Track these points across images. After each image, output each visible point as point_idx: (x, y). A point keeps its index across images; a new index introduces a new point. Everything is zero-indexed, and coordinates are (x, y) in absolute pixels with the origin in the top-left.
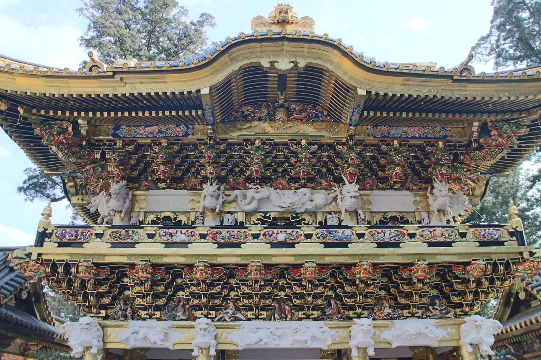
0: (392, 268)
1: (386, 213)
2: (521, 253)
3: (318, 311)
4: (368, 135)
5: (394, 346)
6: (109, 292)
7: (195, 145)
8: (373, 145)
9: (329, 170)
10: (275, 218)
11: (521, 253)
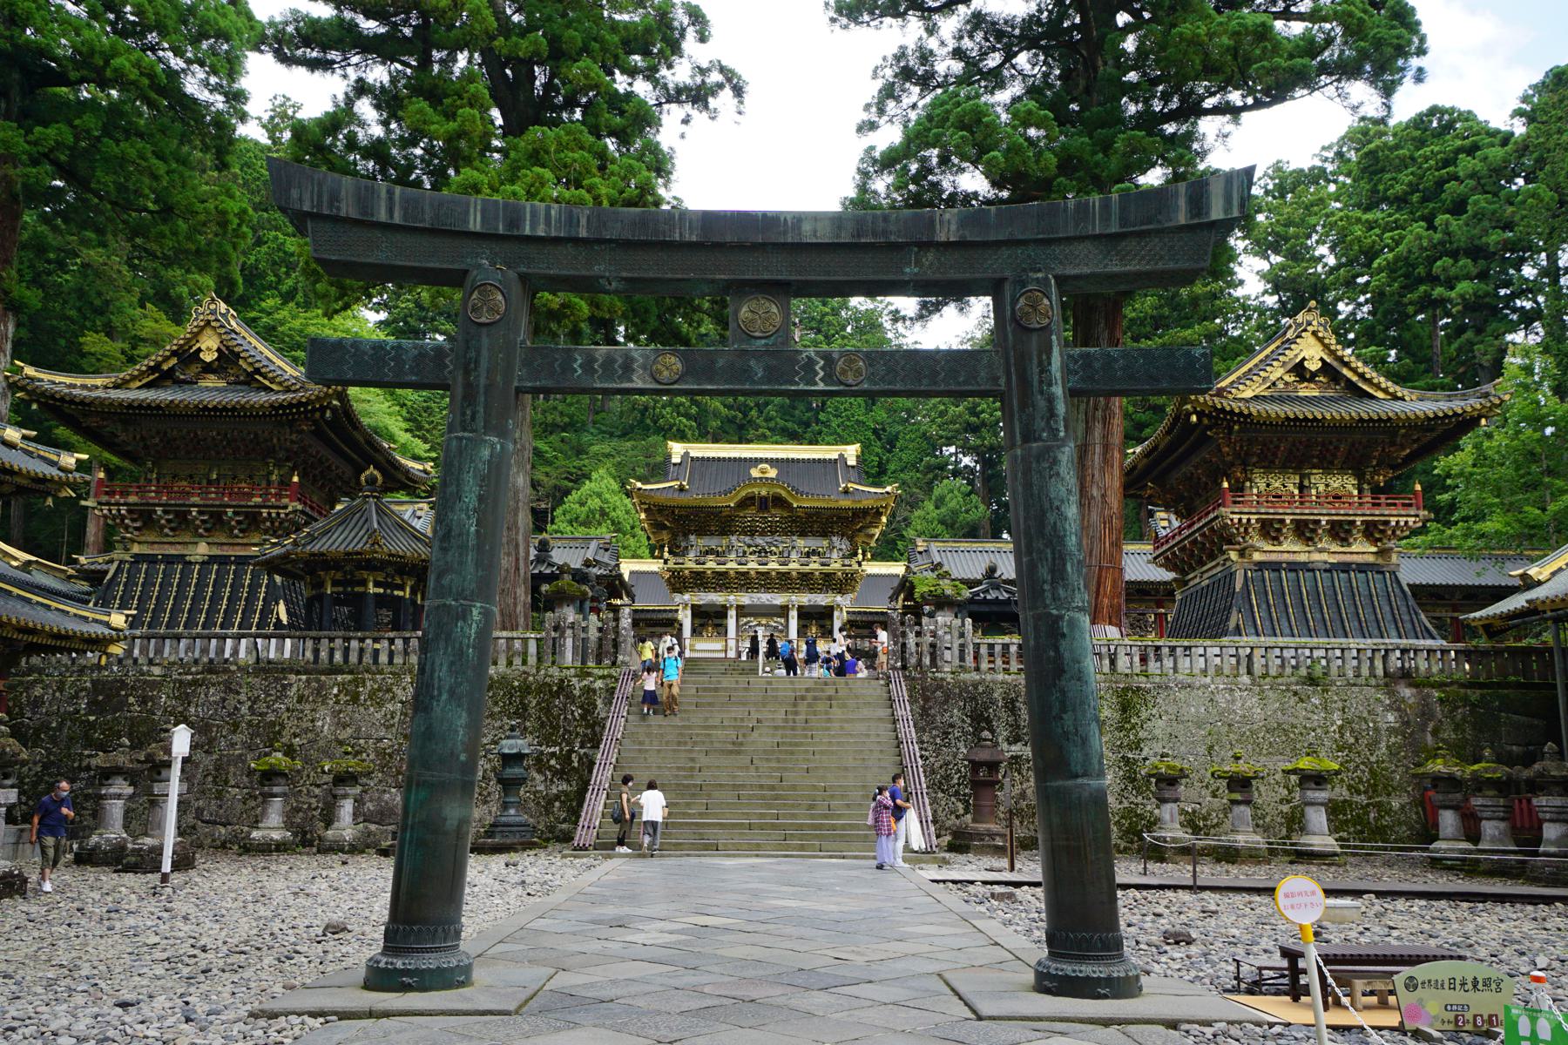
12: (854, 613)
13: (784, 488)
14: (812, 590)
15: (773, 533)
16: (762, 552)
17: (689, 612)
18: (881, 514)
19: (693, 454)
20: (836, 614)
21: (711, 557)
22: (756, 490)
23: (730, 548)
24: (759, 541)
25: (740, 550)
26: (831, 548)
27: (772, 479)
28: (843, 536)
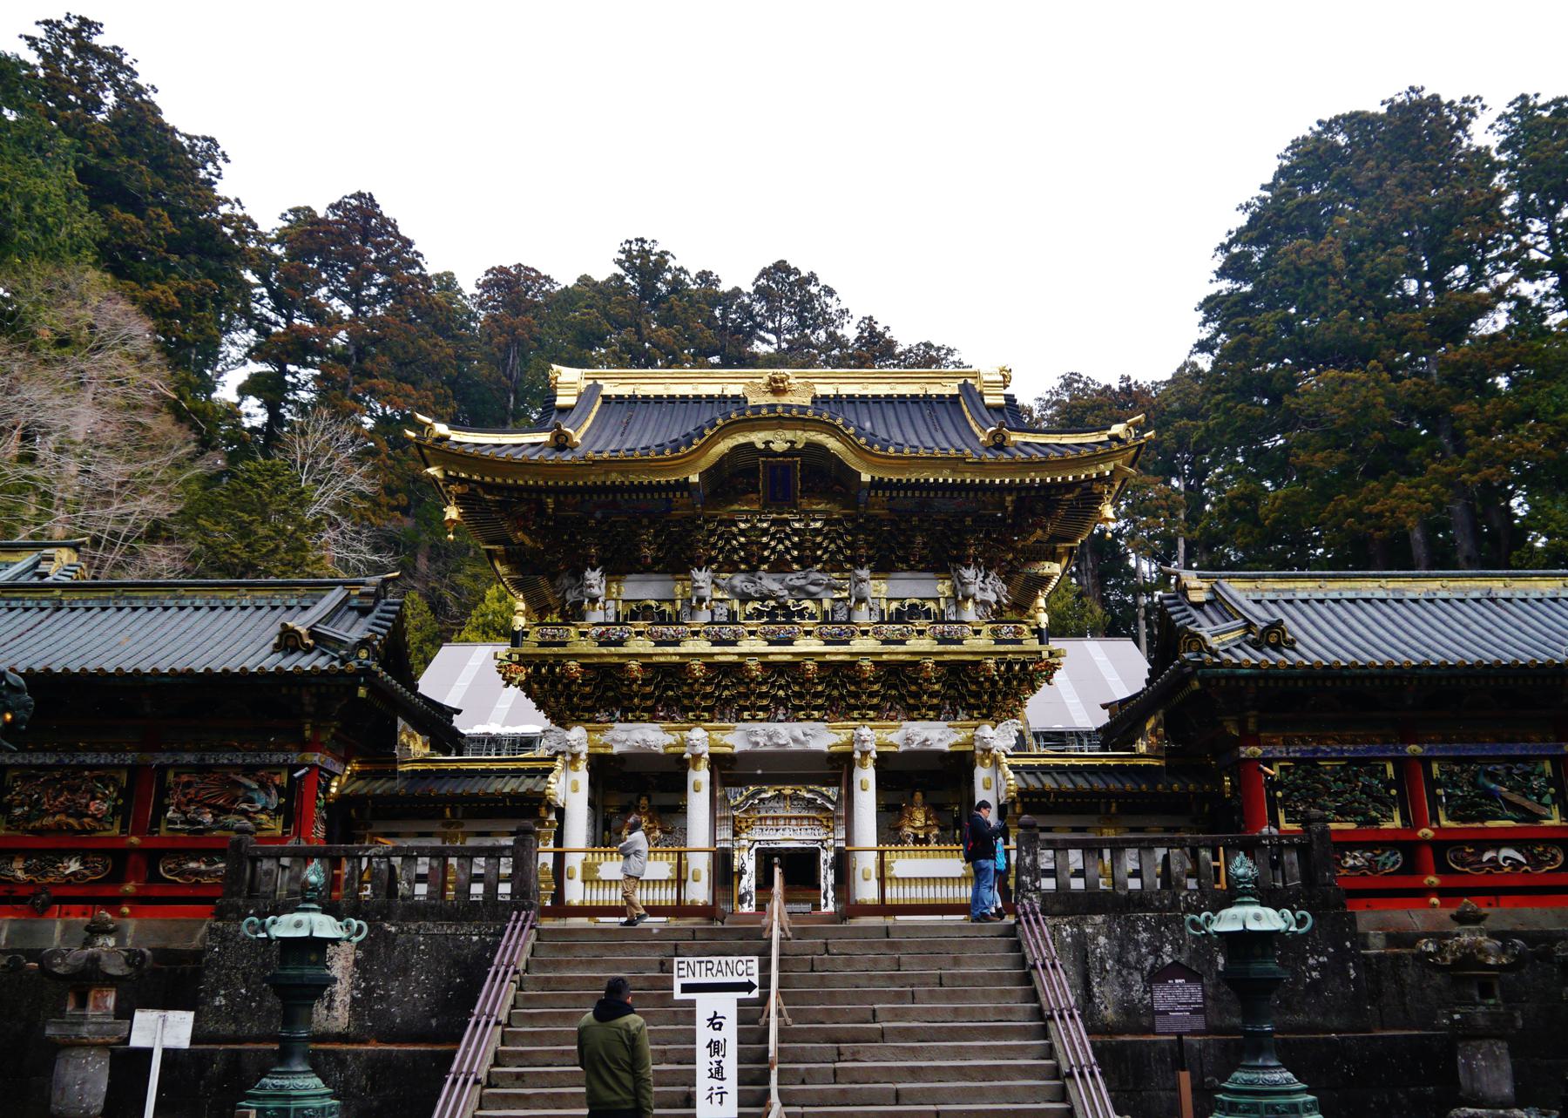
2: (1040, 653)
5: (901, 749)
6: (593, 693)
7: (679, 521)
9: (838, 547)
11: (1040, 653)
12: (1030, 770)
13: (833, 430)
14: (914, 711)
15: (806, 563)
16: (780, 615)
17: (582, 776)
18: (1099, 499)
19: (609, 389)
20: (981, 773)
21: (641, 625)
22: (758, 438)
23: (694, 604)
24: (770, 583)
25: (722, 613)
28: (988, 568)
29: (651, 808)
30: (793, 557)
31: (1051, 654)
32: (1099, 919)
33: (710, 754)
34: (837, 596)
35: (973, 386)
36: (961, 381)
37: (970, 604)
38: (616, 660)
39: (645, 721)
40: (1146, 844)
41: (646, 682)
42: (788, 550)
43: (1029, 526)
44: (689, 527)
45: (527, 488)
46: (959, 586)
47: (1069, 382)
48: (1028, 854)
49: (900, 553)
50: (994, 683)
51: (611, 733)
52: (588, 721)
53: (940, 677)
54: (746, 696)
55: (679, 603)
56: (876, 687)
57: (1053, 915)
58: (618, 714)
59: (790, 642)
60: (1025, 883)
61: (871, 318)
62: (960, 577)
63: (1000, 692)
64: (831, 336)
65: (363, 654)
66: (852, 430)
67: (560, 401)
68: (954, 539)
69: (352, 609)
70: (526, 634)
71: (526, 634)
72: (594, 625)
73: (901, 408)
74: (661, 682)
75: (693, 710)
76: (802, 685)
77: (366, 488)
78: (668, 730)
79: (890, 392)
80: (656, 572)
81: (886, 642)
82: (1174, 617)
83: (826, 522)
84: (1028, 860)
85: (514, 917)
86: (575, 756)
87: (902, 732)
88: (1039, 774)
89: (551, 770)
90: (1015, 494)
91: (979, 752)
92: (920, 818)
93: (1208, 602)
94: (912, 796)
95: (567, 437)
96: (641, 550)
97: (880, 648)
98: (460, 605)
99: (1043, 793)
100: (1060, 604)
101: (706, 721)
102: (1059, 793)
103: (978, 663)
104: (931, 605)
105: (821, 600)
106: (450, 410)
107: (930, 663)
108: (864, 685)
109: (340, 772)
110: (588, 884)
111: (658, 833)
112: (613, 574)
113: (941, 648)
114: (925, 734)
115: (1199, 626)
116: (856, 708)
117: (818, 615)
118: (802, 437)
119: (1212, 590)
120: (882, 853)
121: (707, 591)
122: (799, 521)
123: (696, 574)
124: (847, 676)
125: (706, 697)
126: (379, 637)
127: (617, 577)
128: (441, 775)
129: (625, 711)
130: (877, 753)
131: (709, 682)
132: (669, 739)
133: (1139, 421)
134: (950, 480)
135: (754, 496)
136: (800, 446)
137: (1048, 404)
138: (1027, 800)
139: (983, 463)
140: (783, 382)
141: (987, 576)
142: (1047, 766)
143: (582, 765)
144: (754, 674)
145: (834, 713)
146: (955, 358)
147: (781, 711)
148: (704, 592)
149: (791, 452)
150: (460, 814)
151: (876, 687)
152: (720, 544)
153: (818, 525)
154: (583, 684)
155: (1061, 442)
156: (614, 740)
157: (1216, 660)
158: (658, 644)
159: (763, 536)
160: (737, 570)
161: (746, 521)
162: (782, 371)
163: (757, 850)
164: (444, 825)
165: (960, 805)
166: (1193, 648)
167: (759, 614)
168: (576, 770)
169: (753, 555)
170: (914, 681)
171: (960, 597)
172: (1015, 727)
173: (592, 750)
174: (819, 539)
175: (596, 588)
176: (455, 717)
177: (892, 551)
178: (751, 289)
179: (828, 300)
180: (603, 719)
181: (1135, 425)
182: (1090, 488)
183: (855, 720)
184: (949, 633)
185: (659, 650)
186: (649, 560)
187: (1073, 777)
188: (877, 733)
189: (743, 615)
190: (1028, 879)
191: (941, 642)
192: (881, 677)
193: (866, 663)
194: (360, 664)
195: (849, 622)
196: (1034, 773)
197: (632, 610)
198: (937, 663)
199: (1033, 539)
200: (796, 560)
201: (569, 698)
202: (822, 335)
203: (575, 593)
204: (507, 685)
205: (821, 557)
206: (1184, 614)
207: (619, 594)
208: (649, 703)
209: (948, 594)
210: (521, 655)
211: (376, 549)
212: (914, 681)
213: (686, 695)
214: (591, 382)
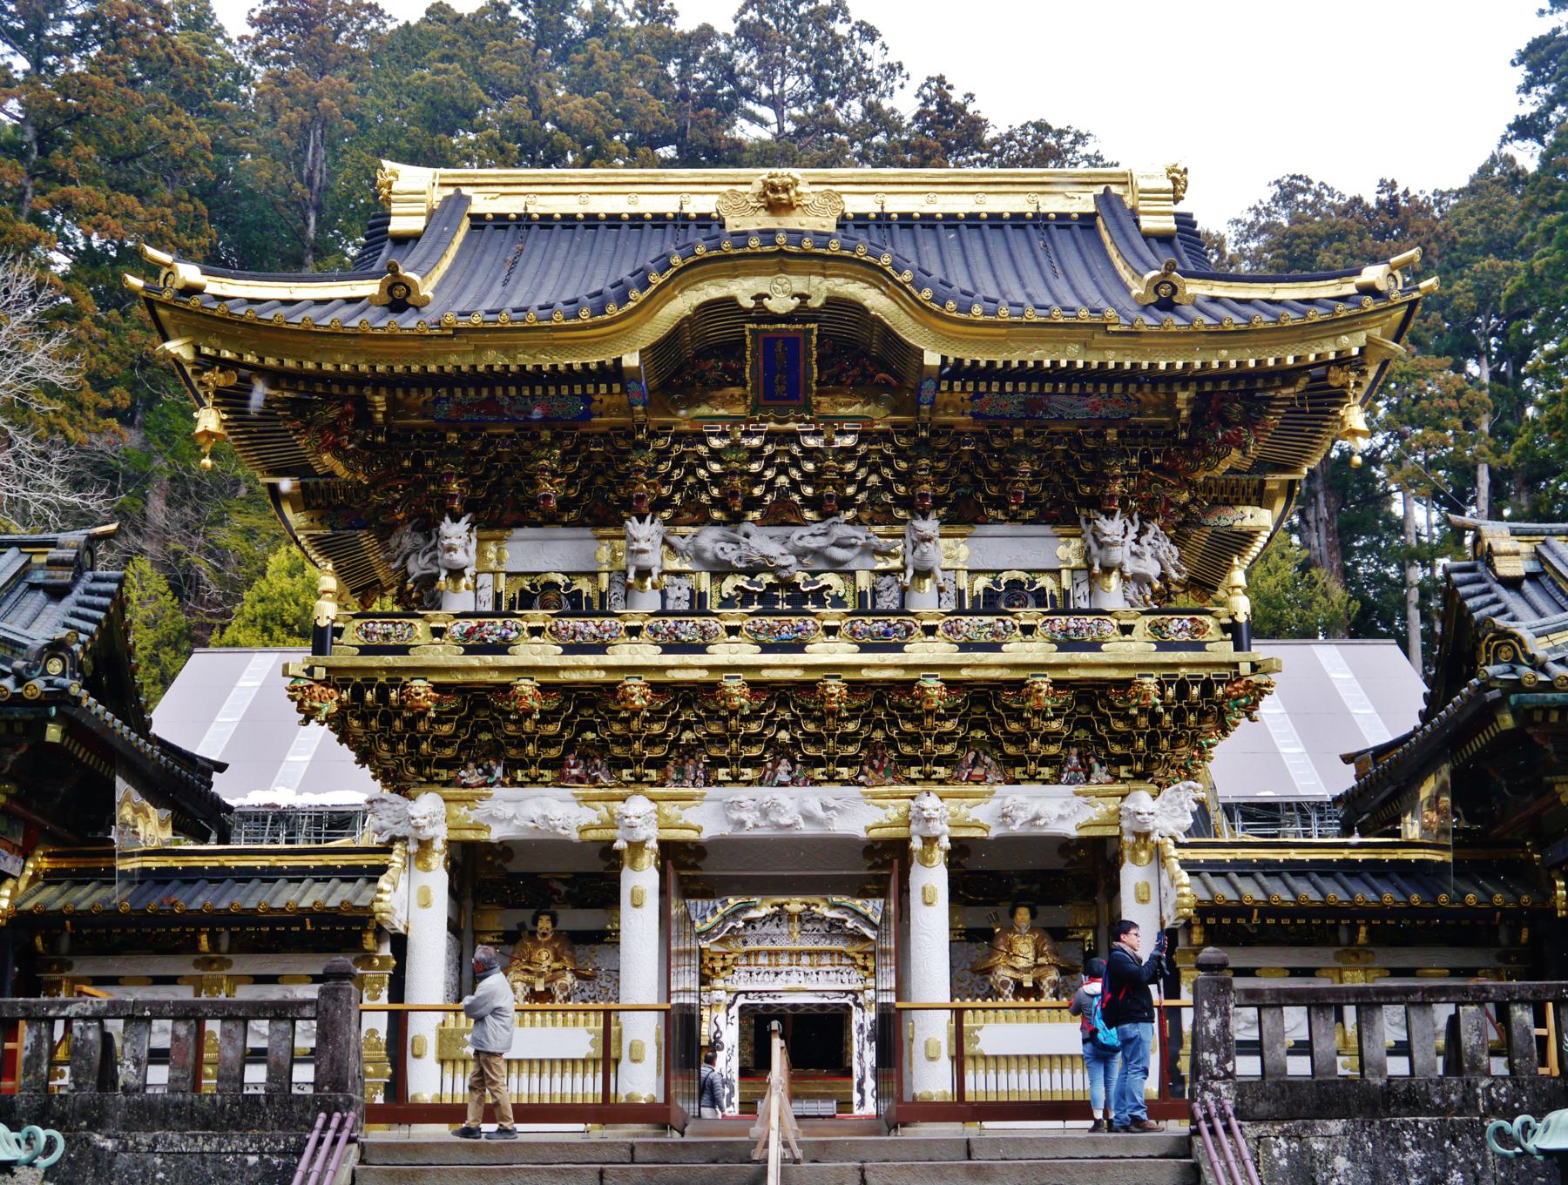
0: (990, 687)
1: (1001, 571)
2: (1236, 665)
3: (850, 767)
4: (963, 414)
5: (994, 833)
6: (455, 736)
7: (602, 435)
8: (973, 433)
9: (884, 480)
10: (769, 585)
11: (1236, 665)
13: (873, 273)
15: (825, 508)
17: (437, 879)
18: (1338, 396)
19: (483, 203)
20: (1132, 876)
21: (538, 617)
22: (743, 290)
24: (764, 542)
25: (679, 597)
26: (1094, 572)
27: (821, 237)
29: (558, 935)
30: (804, 498)
31: (1255, 667)
32: (1336, 1126)
33: (661, 843)
34: (882, 566)
35: (1119, 198)
36: (1100, 190)
37: (1114, 581)
38: (495, 677)
39: (545, 784)
40: (1418, 997)
41: (547, 717)
42: (795, 486)
43: (1219, 444)
44: (622, 444)
45: (338, 378)
46: (1094, 549)
47: (1288, 191)
48: (1213, 1015)
49: (993, 491)
50: (1155, 718)
51: (486, 804)
52: (446, 784)
53: (1061, 709)
54: (723, 741)
55: (604, 578)
56: (949, 726)
57: (1257, 1120)
58: (499, 772)
59: (798, 647)
60: (1207, 1064)
61: (941, 80)
62: (1097, 534)
63: (1165, 734)
64: (872, 110)
65: (55, 666)
66: (907, 276)
67: (397, 225)
68: (1087, 467)
69: (34, 587)
70: (338, 632)
71: (338, 632)
72: (457, 616)
73: (994, 237)
74: (573, 716)
75: (628, 765)
76: (820, 721)
77: (57, 378)
78: (586, 800)
79: (976, 209)
80: (565, 525)
81: (965, 647)
82: (1470, 603)
83: (864, 437)
84: (1213, 1025)
85: (319, 1123)
86: (425, 845)
87: (994, 803)
88: (1233, 876)
89: (383, 869)
90: (1193, 387)
91: (1128, 839)
92: (1025, 949)
93: (1531, 577)
94: (1012, 914)
95: (409, 287)
96: (538, 485)
97: (959, 658)
98: (224, 582)
99: (1241, 909)
100: (1272, 581)
101: (652, 784)
102: (1268, 909)
103: (1128, 683)
104: (1046, 582)
105: (853, 573)
106: (205, 241)
107: (1043, 683)
108: (929, 722)
109: (16, 872)
110: (448, 1066)
111: (569, 978)
112: (490, 526)
113: (1064, 657)
114: (1034, 807)
115: (1513, 619)
116: (914, 761)
117: (849, 599)
118: (820, 288)
119: (1538, 556)
120: (959, 1013)
121: (654, 558)
122: (817, 433)
123: (633, 526)
124: (900, 708)
125: (651, 741)
126: (83, 637)
127: (497, 533)
128: (191, 876)
129: (511, 766)
130: (952, 840)
131: (657, 715)
132: (589, 815)
133: (1411, 260)
134: (1080, 364)
135: (736, 391)
136: (815, 303)
137: (1252, 231)
138: (1211, 921)
139: (1138, 334)
140: (786, 190)
141: (1142, 532)
142: (1248, 863)
143: (438, 861)
144: (737, 702)
145: (877, 771)
146: (1089, 149)
147: (784, 766)
148: (645, 561)
149: (802, 313)
150: (224, 945)
151: (949, 726)
152: (677, 474)
153: (849, 441)
154: (438, 720)
155: (1277, 296)
156: (492, 817)
157: (1542, 678)
158: (569, 650)
159: (751, 460)
160: (707, 521)
161: (723, 435)
162: (786, 171)
163: (742, 1008)
164: (197, 964)
165: (1095, 929)
166: (1502, 656)
167: (746, 597)
168: (427, 869)
169: (734, 494)
170: (1017, 715)
171: (1097, 569)
172: (1192, 795)
173: (455, 835)
174: (850, 467)
175: (461, 552)
176: (216, 777)
177: (977, 485)
178: (731, 28)
179: (867, 47)
180: (473, 781)
181: (1404, 267)
182: (1325, 378)
183: (913, 782)
184: (1077, 630)
185: (571, 660)
186: (553, 503)
187: (1291, 880)
188: (951, 806)
189: (717, 600)
190: (1214, 1058)
191: (1063, 646)
192: (956, 708)
193: (931, 683)
194: (49, 683)
195: (902, 611)
196: (1224, 875)
197: (523, 591)
198: (1057, 684)
199: (1224, 466)
200: (809, 503)
201: (414, 743)
202: (855, 108)
203: (423, 561)
204: (306, 721)
205: (853, 497)
206: (1487, 598)
207: (499, 562)
208: (554, 753)
209: (1076, 562)
210: (328, 669)
211: (77, 484)
212: (1017, 715)
213: (616, 740)
214: (450, 191)
